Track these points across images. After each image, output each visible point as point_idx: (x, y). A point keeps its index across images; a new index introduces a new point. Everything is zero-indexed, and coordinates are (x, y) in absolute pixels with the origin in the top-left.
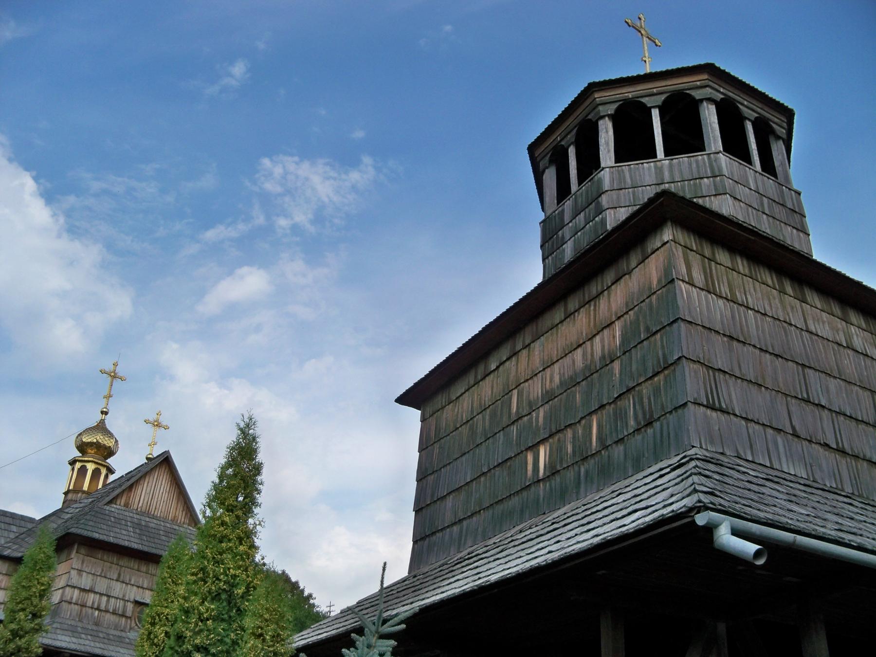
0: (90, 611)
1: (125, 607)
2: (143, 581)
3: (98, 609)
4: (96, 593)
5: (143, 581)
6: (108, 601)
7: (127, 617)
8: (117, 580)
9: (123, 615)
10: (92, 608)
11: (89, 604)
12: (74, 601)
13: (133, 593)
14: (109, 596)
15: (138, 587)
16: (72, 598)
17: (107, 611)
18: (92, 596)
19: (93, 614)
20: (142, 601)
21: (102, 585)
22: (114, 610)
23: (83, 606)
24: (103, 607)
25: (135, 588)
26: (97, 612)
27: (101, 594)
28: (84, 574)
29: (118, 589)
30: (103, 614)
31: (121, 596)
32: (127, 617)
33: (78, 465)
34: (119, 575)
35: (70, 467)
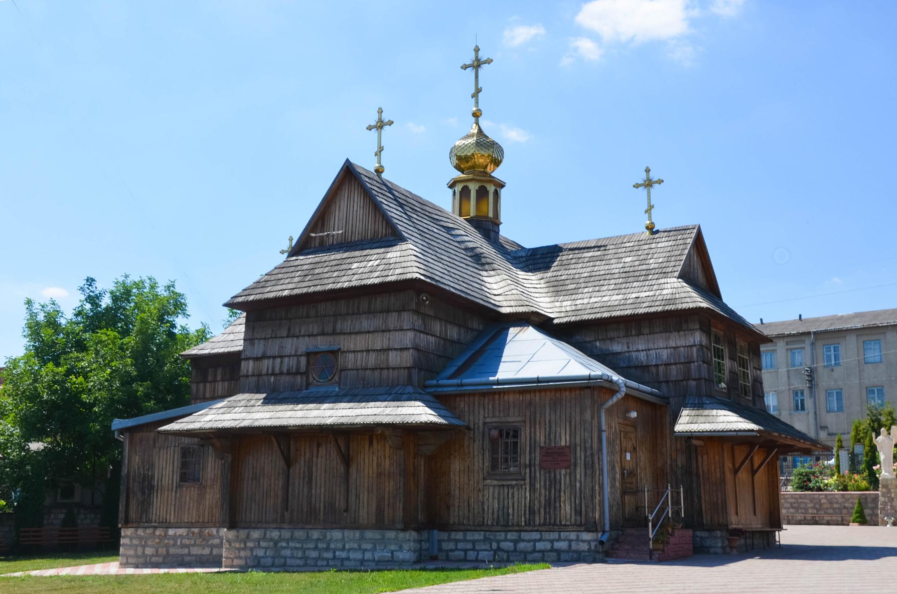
0: (266, 378)
1: (299, 362)
2: (313, 328)
3: (273, 374)
4: (269, 357)
5: (313, 328)
6: (282, 363)
7: (302, 374)
8: (288, 337)
9: (298, 373)
10: (267, 375)
11: (264, 372)
12: (250, 373)
13: (304, 345)
14: (281, 357)
15: (309, 336)
16: (248, 371)
17: (281, 373)
18: (266, 361)
19: (269, 380)
20: (317, 350)
21: (274, 348)
22: (288, 370)
23: (260, 375)
24: (277, 370)
25: (307, 338)
26: (272, 379)
27: (274, 357)
28: (256, 341)
29: (290, 345)
30: (278, 377)
31: (293, 353)
32: (302, 374)
33: (458, 188)
34: (289, 330)
35: (451, 191)
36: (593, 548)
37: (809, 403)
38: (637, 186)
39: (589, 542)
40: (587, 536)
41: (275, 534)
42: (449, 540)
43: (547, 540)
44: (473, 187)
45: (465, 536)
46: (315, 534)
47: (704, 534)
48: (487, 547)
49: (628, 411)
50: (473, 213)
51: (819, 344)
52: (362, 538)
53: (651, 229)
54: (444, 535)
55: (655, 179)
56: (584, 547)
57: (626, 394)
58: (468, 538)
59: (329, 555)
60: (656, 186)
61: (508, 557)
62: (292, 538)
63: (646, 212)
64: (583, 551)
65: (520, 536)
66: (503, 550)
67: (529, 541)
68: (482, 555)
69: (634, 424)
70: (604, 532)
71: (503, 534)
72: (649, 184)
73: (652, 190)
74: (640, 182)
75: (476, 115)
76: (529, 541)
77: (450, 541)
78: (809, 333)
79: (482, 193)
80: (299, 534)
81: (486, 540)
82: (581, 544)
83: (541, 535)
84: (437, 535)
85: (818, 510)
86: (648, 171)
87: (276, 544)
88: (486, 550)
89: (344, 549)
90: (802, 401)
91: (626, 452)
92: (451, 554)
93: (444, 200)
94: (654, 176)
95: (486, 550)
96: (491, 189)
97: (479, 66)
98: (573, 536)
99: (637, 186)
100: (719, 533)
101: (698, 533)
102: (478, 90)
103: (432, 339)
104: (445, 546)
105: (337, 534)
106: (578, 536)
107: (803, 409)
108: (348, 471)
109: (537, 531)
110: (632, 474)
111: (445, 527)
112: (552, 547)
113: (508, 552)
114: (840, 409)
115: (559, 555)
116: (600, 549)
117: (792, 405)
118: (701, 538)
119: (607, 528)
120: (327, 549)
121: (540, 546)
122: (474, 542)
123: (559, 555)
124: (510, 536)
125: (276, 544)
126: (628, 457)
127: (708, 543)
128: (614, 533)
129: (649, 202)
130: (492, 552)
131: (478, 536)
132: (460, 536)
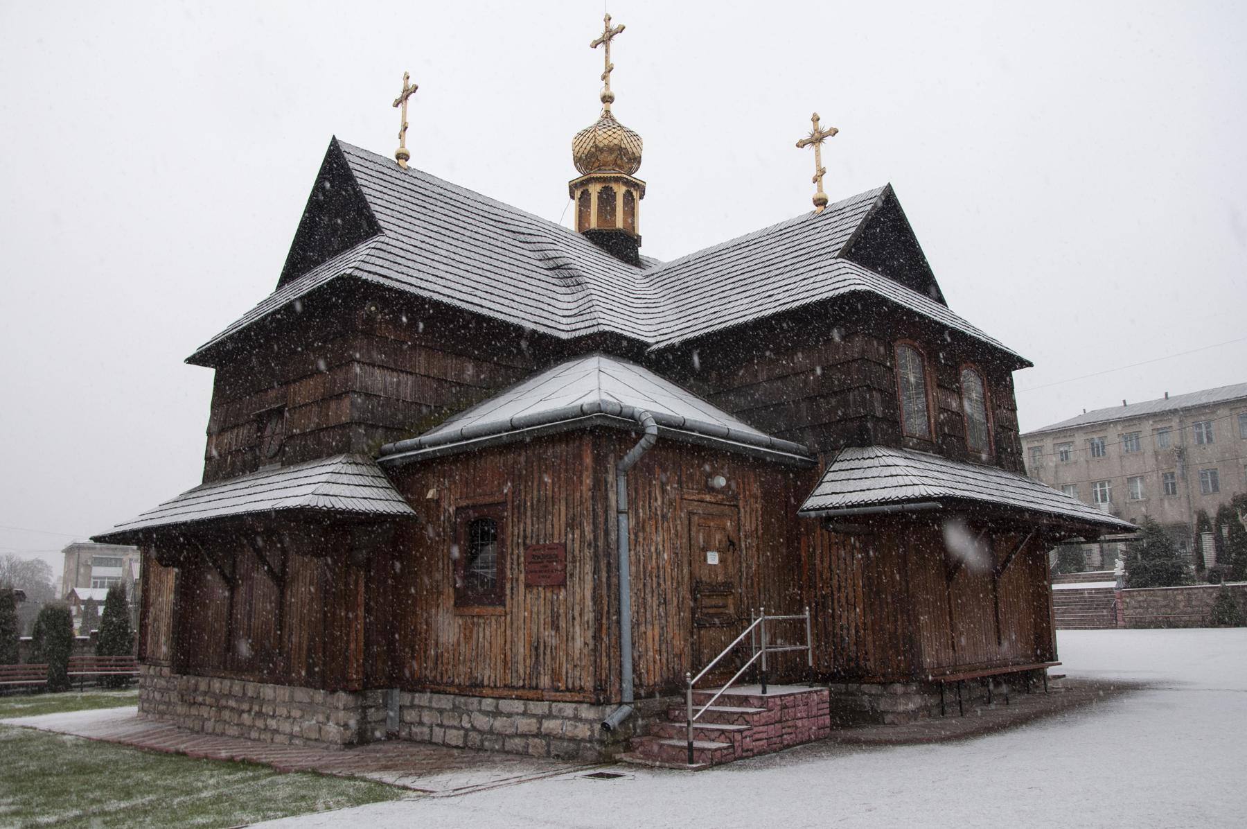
33: (578, 194)
36: (597, 735)
37: (1181, 488)
38: (801, 145)
39: (591, 722)
40: (587, 712)
41: (216, 685)
42: (412, 706)
43: (534, 716)
44: (594, 190)
45: (430, 700)
46: (251, 689)
47: (875, 689)
48: (456, 723)
49: (711, 475)
50: (593, 223)
51: (1189, 422)
52: (292, 700)
53: (821, 202)
54: (406, 698)
55: (827, 129)
56: (583, 731)
57: (661, 439)
58: (434, 705)
59: (260, 723)
60: (828, 140)
61: (482, 741)
62: (229, 696)
63: (815, 180)
64: (583, 740)
65: (497, 707)
66: (474, 728)
67: (509, 715)
68: (454, 737)
69: (731, 499)
70: (621, 704)
71: (475, 700)
72: (817, 139)
73: (823, 146)
74: (806, 136)
75: (607, 99)
76: (509, 715)
77: (427, 712)
78: (1176, 410)
79: (607, 198)
80: (237, 688)
81: (455, 708)
82: (580, 725)
83: (525, 705)
84: (400, 697)
85: (1172, 609)
86: (816, 119)
87: (217, 700)
88: (455, 727)
89: (273, 717)
90: (1173, 484)
91: (705, 549)
92: (414, 729)
93: (564, 214)
94: (824, 125)
95: (455, 727)
96: (620, 190)
97: (610, 38)
98: (569, 709)
99: (801, 145)
100: (899, 688)
101: (865, 688)
102: (609, 70)
103: (410, 380)
104: (410, 716)
105: (268, 691)
106: (576, 709)
107: (1174, 492)
108: (282, 593)
109: (519, 698)
110: (725, 589)
111: (415, 685)
112: (539, 729)
113: (481, 732)
114: (1216, 488)
115: (548, 745)
116: (607, 737)
117: (1163, 487)
118: (871, 695)
119: (628, 695)
120: (260, 714)
121: (525, 724)
122: (441, 711)
123: (548, 745)
124: (488, 704)
125: (217, 700)
126: (713, 558)
127: (883, 705)
128: (657, 702)
129: (818, 164)
130: (462, 732)
131: (445, 702)
132: (422, 699)
